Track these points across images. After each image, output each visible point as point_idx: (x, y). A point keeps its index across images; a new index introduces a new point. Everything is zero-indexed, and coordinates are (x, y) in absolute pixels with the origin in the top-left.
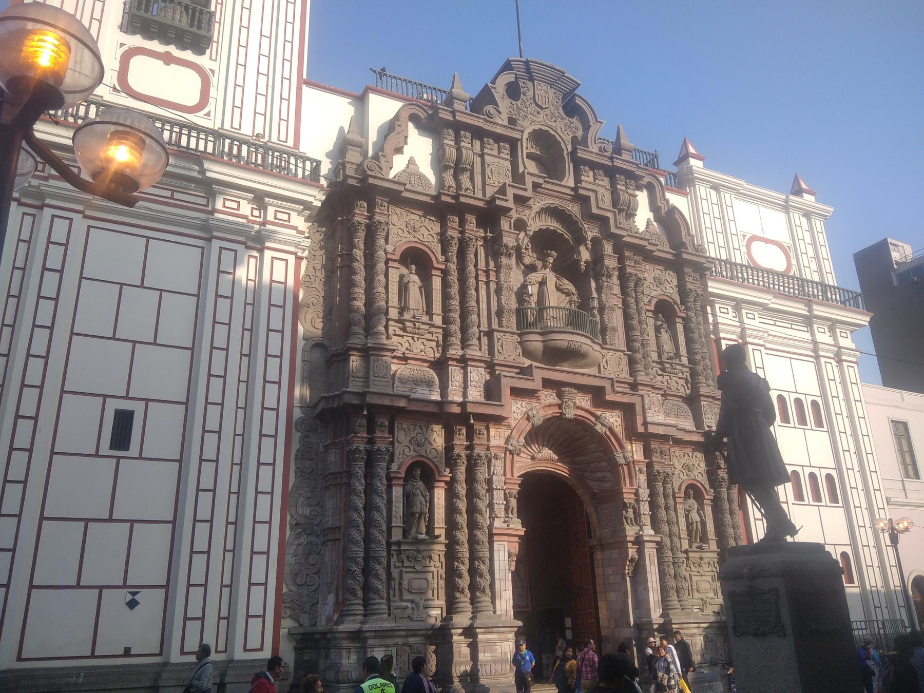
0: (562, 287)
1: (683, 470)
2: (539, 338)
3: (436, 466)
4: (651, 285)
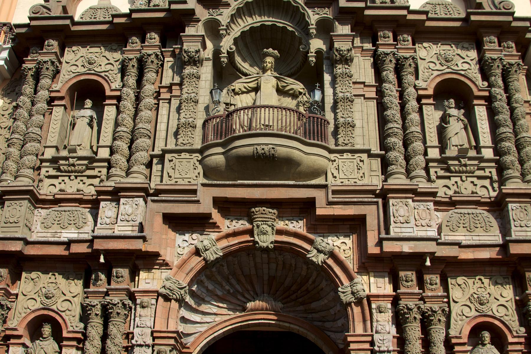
0: (288, 88)
1: (468, 303)
2: (220, 150)
3: (64, 320)
4: (432, 65)
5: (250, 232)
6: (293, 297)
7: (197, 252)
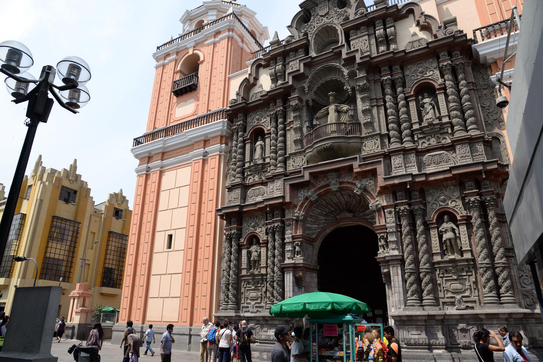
1: (436, 202)
5: (328, 185)
6: (358, 209)
7: (307, 198)
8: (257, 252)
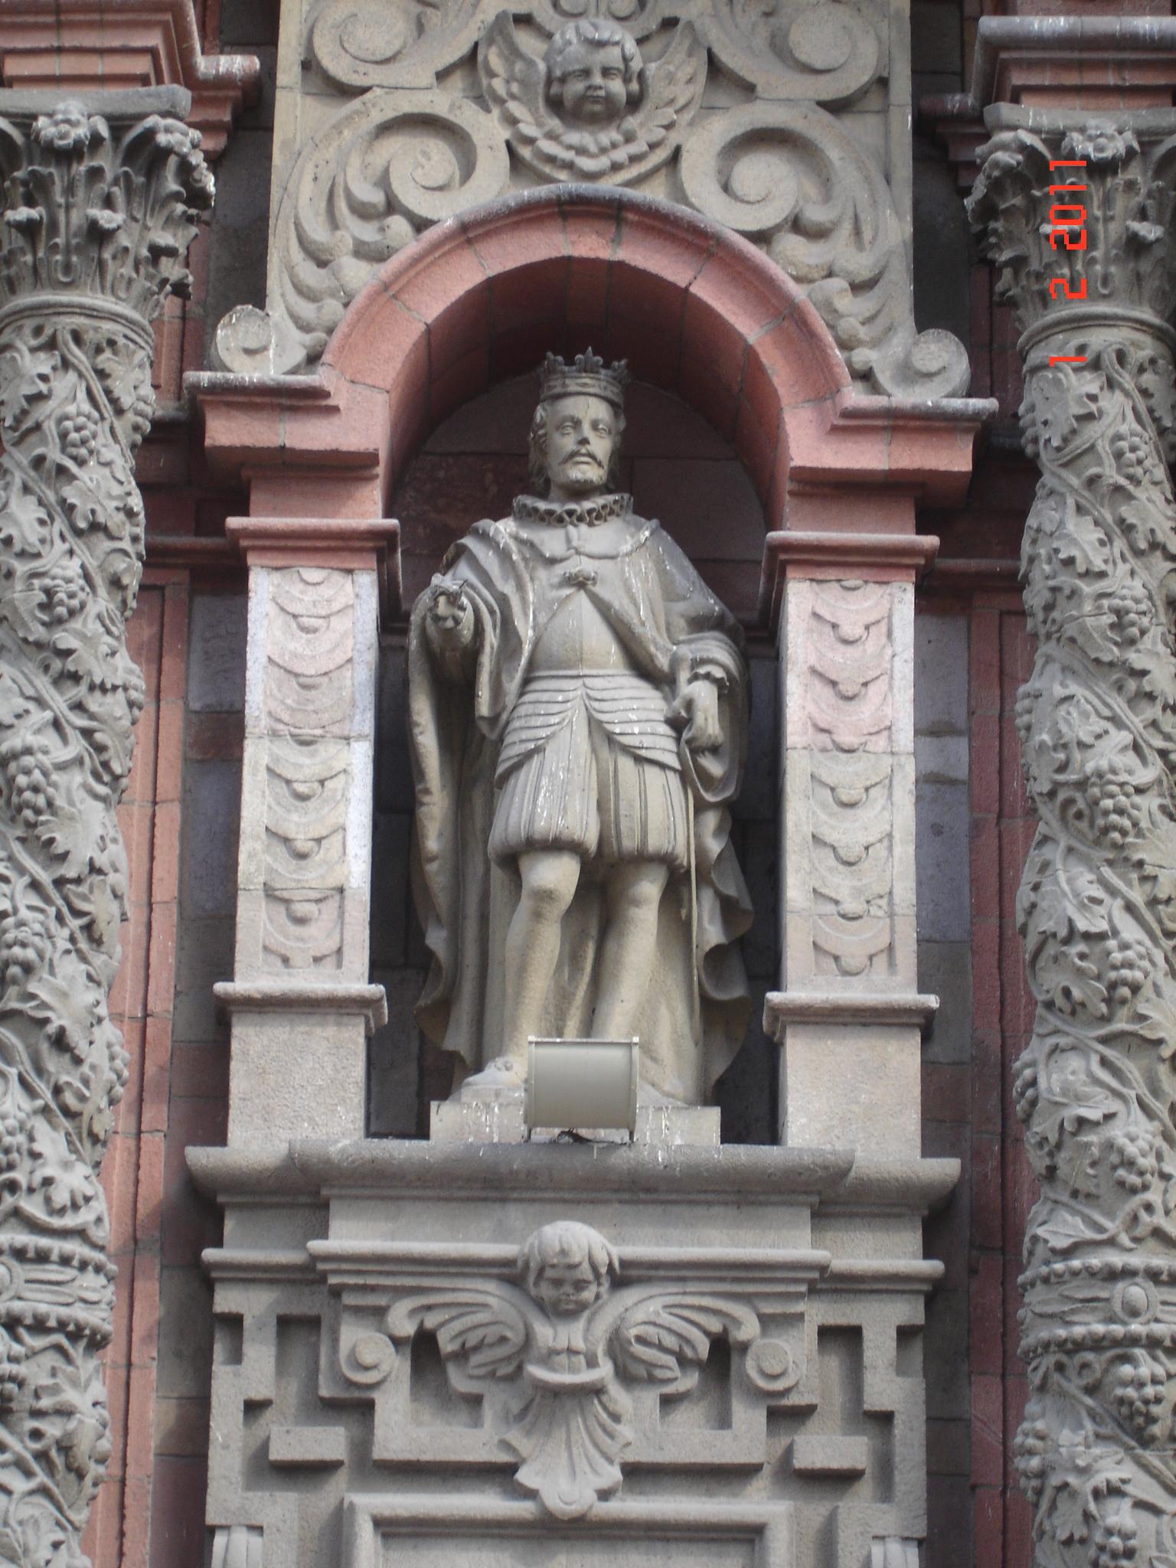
8: (660, 679)
